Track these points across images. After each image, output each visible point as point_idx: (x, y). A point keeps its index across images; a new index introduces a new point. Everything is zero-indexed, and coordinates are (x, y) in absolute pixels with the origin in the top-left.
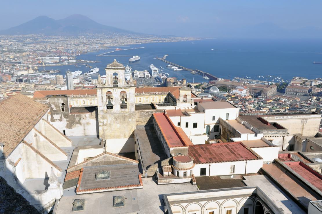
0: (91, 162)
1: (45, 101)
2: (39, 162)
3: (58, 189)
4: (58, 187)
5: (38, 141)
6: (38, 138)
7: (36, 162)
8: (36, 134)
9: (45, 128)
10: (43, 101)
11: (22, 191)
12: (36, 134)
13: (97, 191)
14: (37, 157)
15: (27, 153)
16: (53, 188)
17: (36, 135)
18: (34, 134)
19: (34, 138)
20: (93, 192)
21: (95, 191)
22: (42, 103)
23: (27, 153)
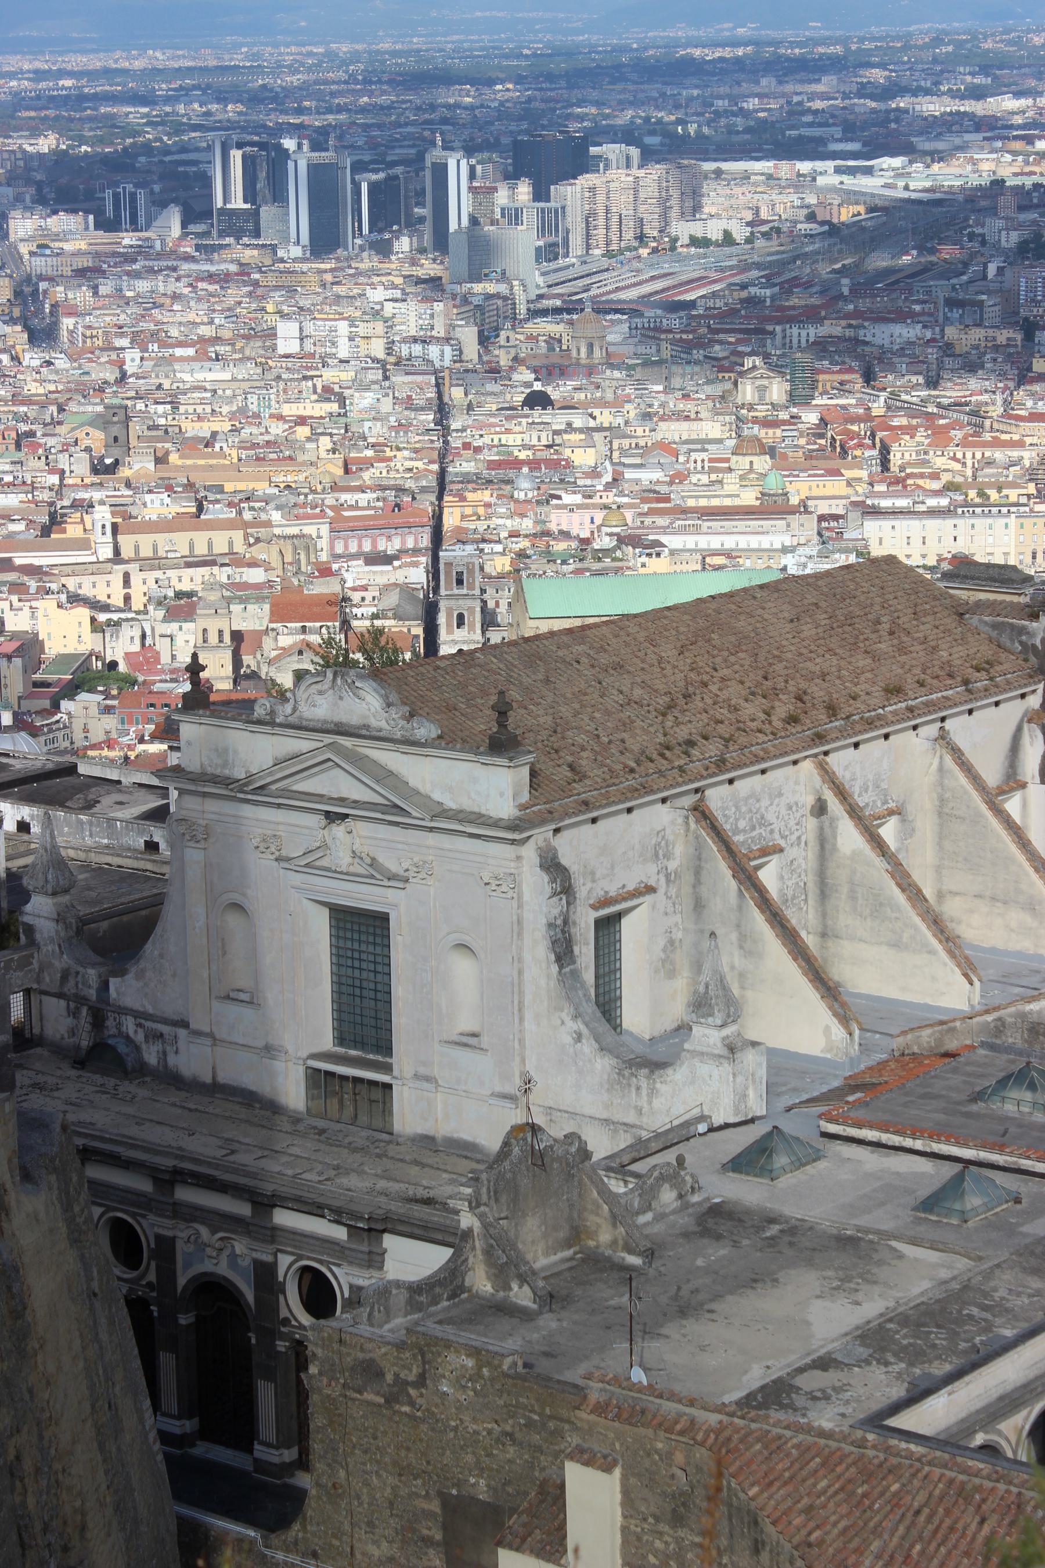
0: (1023, 1016)
1: (1022, 631)
2: (746, 943)
3: (727, 1068)
4: (725, 1052)
5: (828, 847)
6: (827, 830)
7: (734, 936)
8: (819, 800)
9: (942, 800)
10: (1012, 625)
11: (575, 1027)
12: (819, 800)
13: (918, 1145)
14: (740, 908)
15: (698, 871)
16: (702, 1054)
17: (820, 809)
18: (810, 800)
19: (811, 823)
20: (896, 1140)
21: (908, 1143)
22: (1005, 640)
23: (698, 871)
